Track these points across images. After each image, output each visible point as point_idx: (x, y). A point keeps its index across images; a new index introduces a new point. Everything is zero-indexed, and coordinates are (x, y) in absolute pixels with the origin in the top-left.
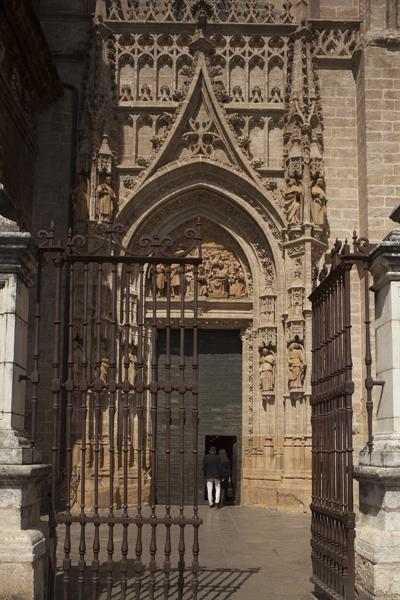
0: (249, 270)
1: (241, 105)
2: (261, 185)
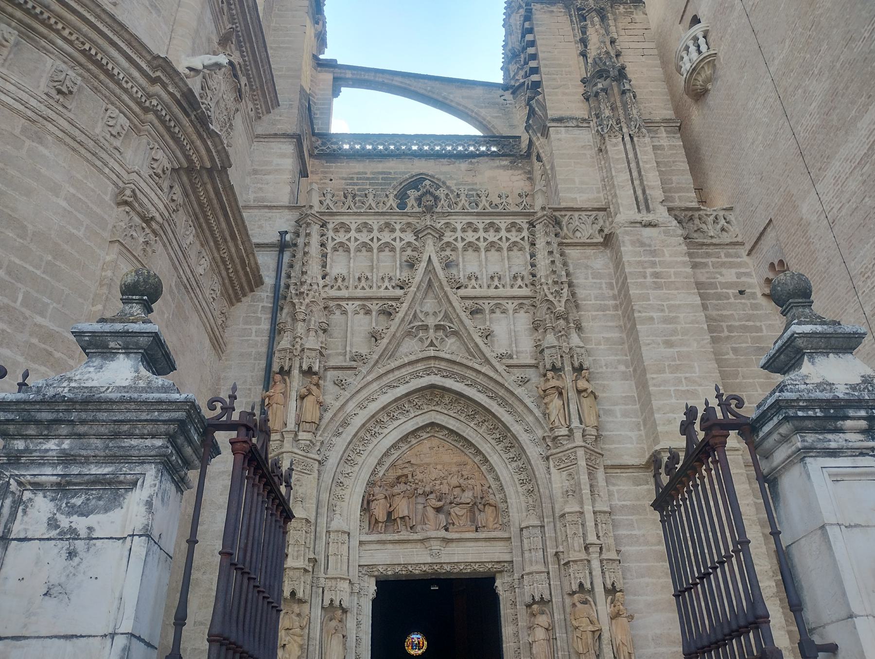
1: (478, 292)
2: (510, 380)
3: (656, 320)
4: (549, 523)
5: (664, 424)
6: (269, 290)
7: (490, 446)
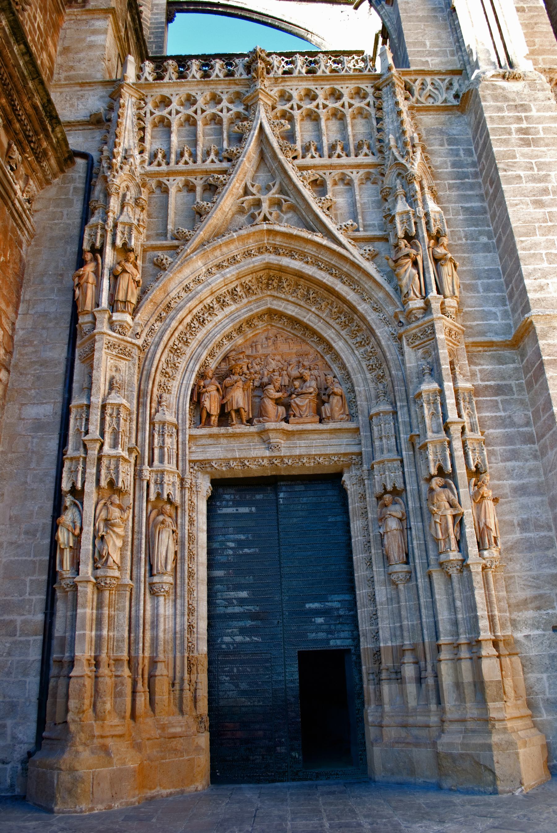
3: (523, 179)
4: (402, 407)
5: (535, 291)
6: (81, 170)
7: (334, 331)
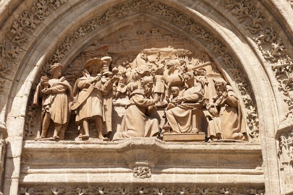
0: (247, 86)
